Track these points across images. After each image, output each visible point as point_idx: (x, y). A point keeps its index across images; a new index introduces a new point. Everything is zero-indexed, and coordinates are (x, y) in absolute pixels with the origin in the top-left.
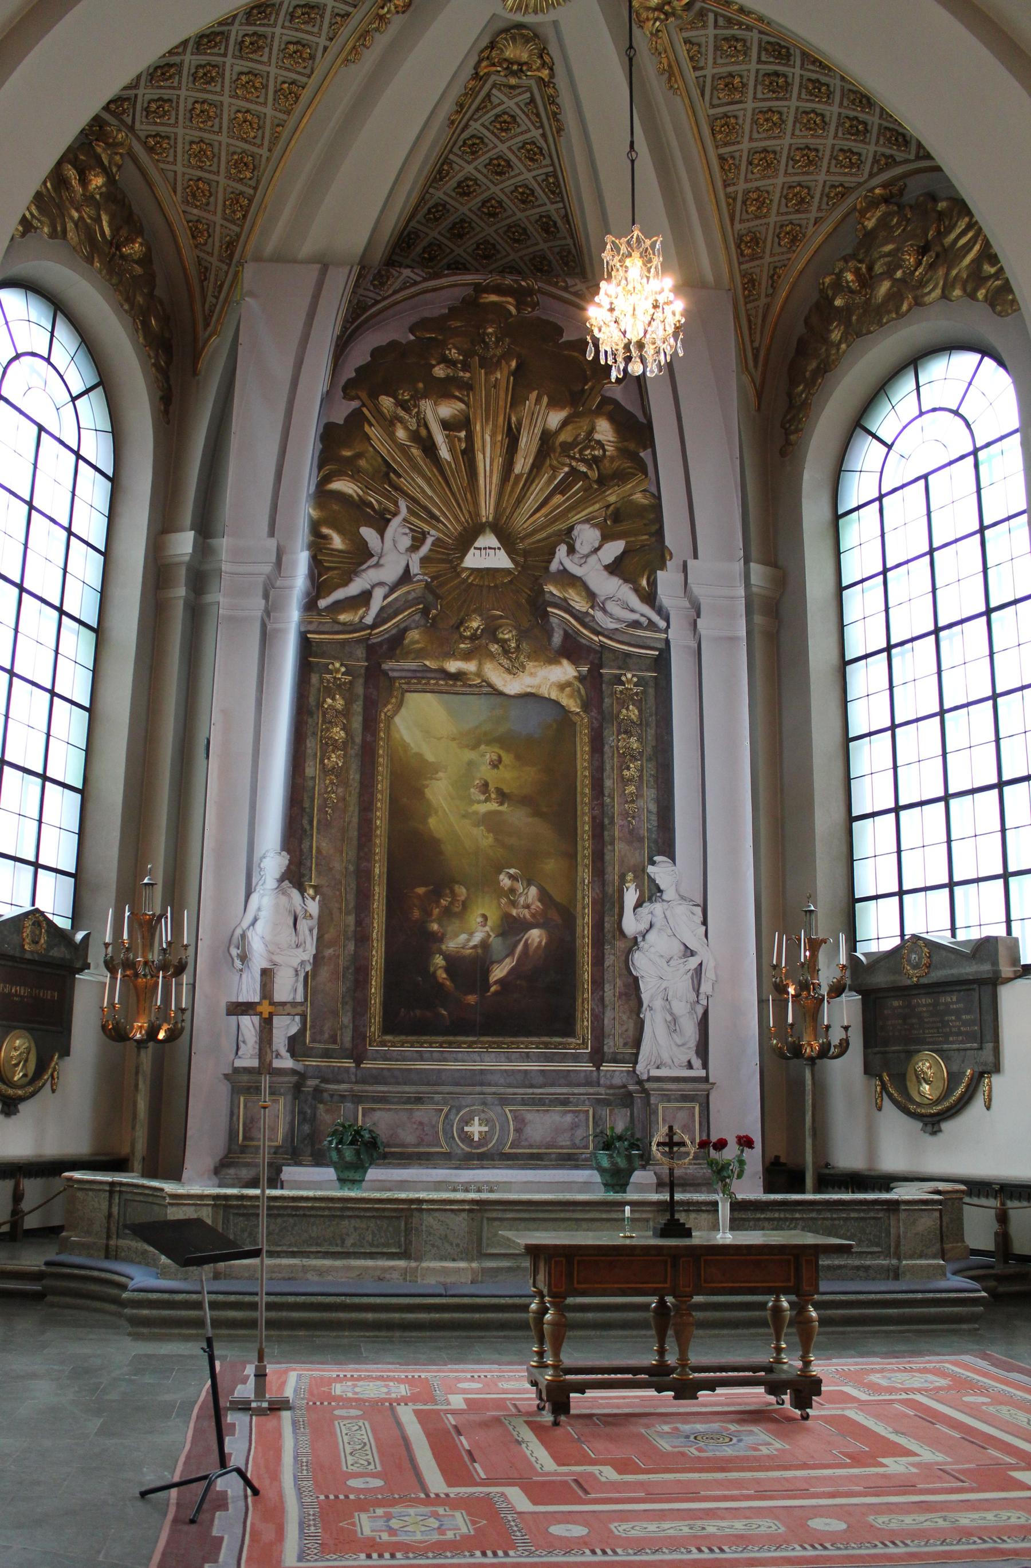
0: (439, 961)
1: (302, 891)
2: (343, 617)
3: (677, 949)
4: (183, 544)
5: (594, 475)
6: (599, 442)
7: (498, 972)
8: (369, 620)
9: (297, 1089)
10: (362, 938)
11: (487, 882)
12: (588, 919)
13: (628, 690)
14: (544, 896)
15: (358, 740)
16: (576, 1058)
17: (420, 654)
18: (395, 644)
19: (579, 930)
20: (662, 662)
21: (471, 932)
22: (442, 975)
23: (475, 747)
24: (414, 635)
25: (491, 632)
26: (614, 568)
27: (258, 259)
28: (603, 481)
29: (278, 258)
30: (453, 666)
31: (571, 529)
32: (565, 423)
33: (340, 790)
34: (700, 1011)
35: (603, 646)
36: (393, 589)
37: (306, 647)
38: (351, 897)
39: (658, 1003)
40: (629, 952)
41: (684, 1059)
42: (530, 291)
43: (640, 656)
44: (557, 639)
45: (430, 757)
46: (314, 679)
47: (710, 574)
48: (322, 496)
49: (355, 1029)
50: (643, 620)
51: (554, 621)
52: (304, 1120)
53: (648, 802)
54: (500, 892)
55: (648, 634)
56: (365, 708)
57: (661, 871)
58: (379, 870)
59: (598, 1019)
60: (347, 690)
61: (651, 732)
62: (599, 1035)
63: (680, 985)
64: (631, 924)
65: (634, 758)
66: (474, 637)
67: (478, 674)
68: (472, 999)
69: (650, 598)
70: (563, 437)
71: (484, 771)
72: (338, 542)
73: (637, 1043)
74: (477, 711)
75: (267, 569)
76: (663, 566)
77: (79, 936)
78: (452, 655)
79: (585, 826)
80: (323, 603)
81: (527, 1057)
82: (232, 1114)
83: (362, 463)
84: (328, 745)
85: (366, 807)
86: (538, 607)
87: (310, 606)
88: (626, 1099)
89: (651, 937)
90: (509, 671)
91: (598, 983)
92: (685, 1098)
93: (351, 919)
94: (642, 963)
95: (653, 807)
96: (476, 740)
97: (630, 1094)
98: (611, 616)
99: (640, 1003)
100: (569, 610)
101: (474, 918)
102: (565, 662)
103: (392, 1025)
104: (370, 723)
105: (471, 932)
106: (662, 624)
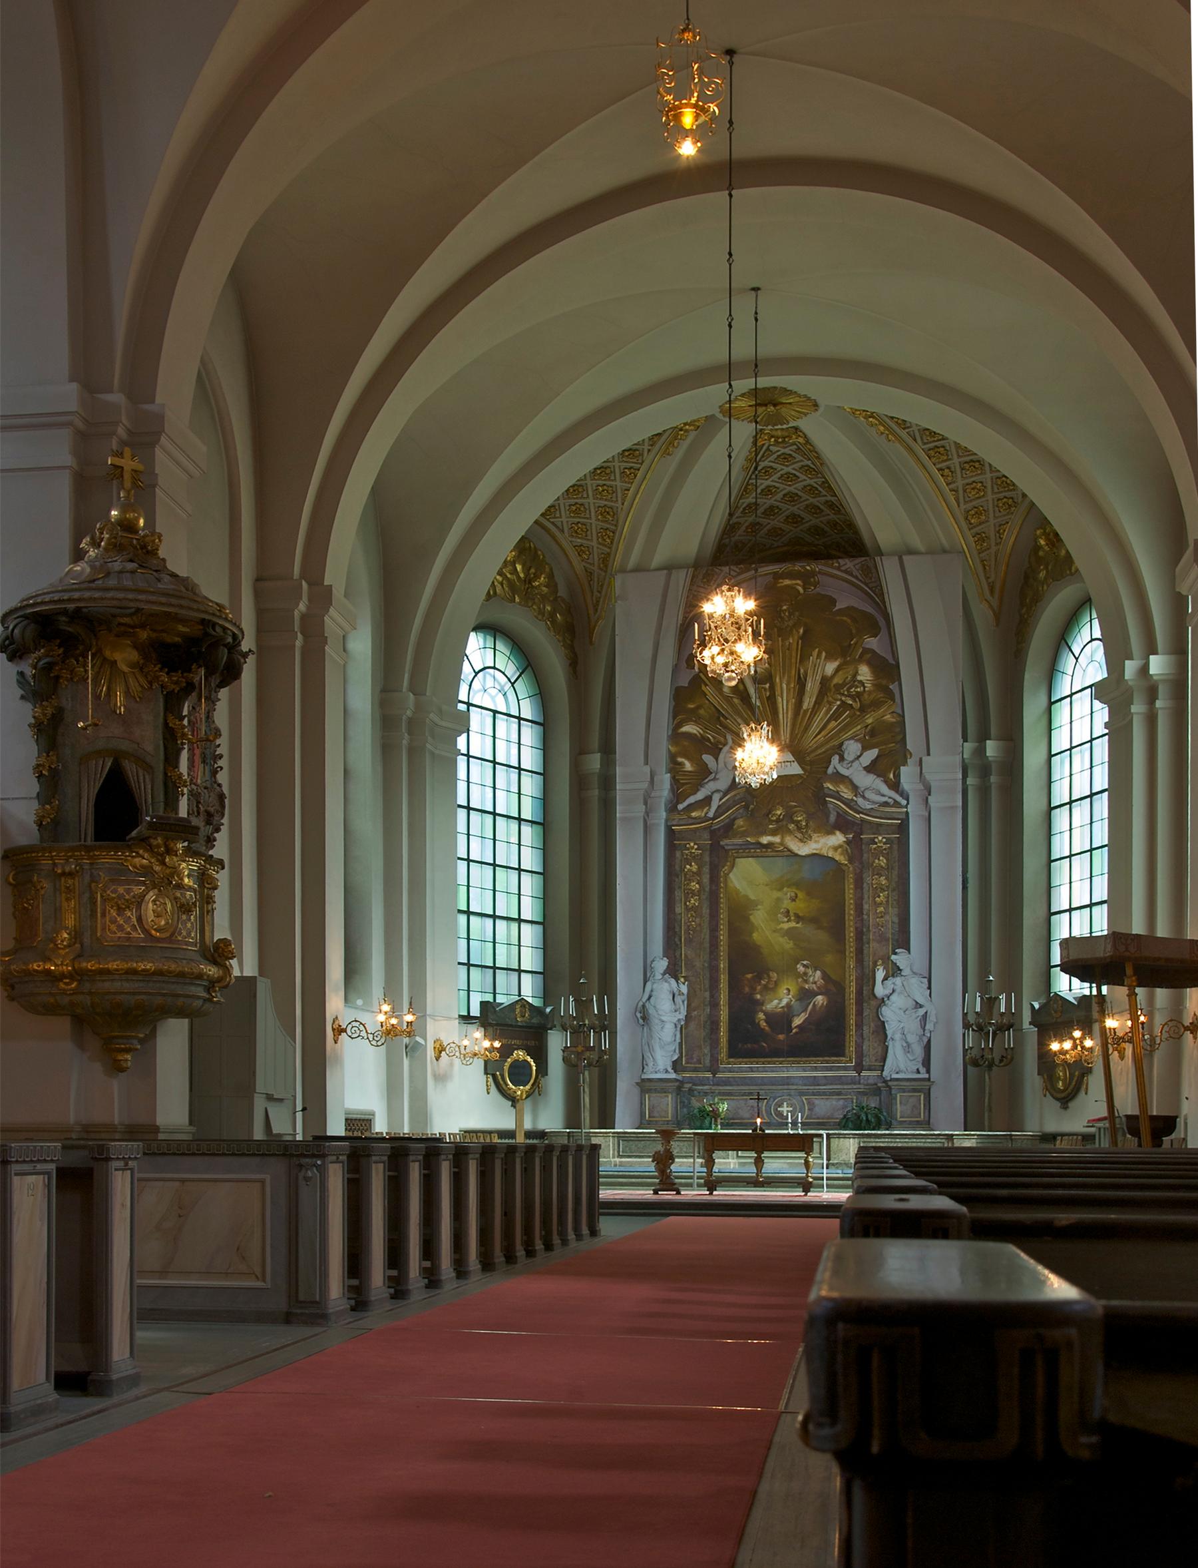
0: (761, 1016)
1: (677, 980)
2: (693, 814)
3: (911, 1003)
4: (594, 762)
5: (857, 705)
6: (861, 682)
7: (797, 1021)
8: (711, 815)
9: (679, 1089)
10: (714, 1005)
11: (790, 970)
12: (853, 989)
13: (880, 846)
14: (825, 976)
15: (707, 889)
16: (845, 1069)
17: (745, 834)
18: (728, 828)
19: (847, 995)
20: (903, 828)
21: (781, 998)
22: (763, 1024)
23: (780, 889)
24: (740, 822)
25: (789, 817)
26: (870, 769)
27: (623, 570)
28: (863, 709)
29: (638, 569)
30: (765, 840)
31: (842, 744)
32: (837, 670)
33: (698, 920)
34: (925, 1040)
35: (862, 820)
36: (725, 794)
37: (671, 834)
38: (707, 982)
39: (898, 1036)
40: (879, 1006)
41: (915, 1068)
42: (813, 574)
43: (888, 825)
44: (833, 818)
45: (753, 897)
46: (678, 854)
47: (939, 762)
48: (676, 736)
49: (712, 1056)
50: (890, 800)
51: (830, 806)
52: (683, 1105)
53: (892, 917)
54: (798, 975)
55: (894, 810)
56: (711, 870)
57: (900, 959)
58: (723, 965)
59: (859, 1047)
60: (697, 859)
61: (895, 872)
62: (860, 1055)
63: (913, 1025)
64: (880, 990)
65: (883, 890)
66: (778, 821)
67: (781, 844)
68: (781, 1037)
69: (895, 786)
70: (836, 681)
71: (787, 904)
72: (688, 766)
73: (884, 1059)
74: (780, 866)
75: (645, 785)
76: (905, 763)
77: (548, 1010)
78: (764, 833)
79: (850, 934)
80: (680, 807)
81: (816, 1069)
82: (642, 1104)
83: (702, 712)
84: (689, 893)
85: (714, 930)
86: (820, 798)
87: (672, 809)
88: (877, 1091)
89: (894, 998)
90: (801, 841)
91: (859, 1026)
92: (915, 1090)
93: (707, 994)
94: (887, 1013)
95: (896, 920)
96: (780, 885)
97: (879, 1088)
98: (868, 800)
99: (886, 1036)
100: (840, 798)
101: (782, 991)
102: (838, 833)
103: (735, 1052)
104: (714, 879)
105: (781, 998)
106: (904, 802)
